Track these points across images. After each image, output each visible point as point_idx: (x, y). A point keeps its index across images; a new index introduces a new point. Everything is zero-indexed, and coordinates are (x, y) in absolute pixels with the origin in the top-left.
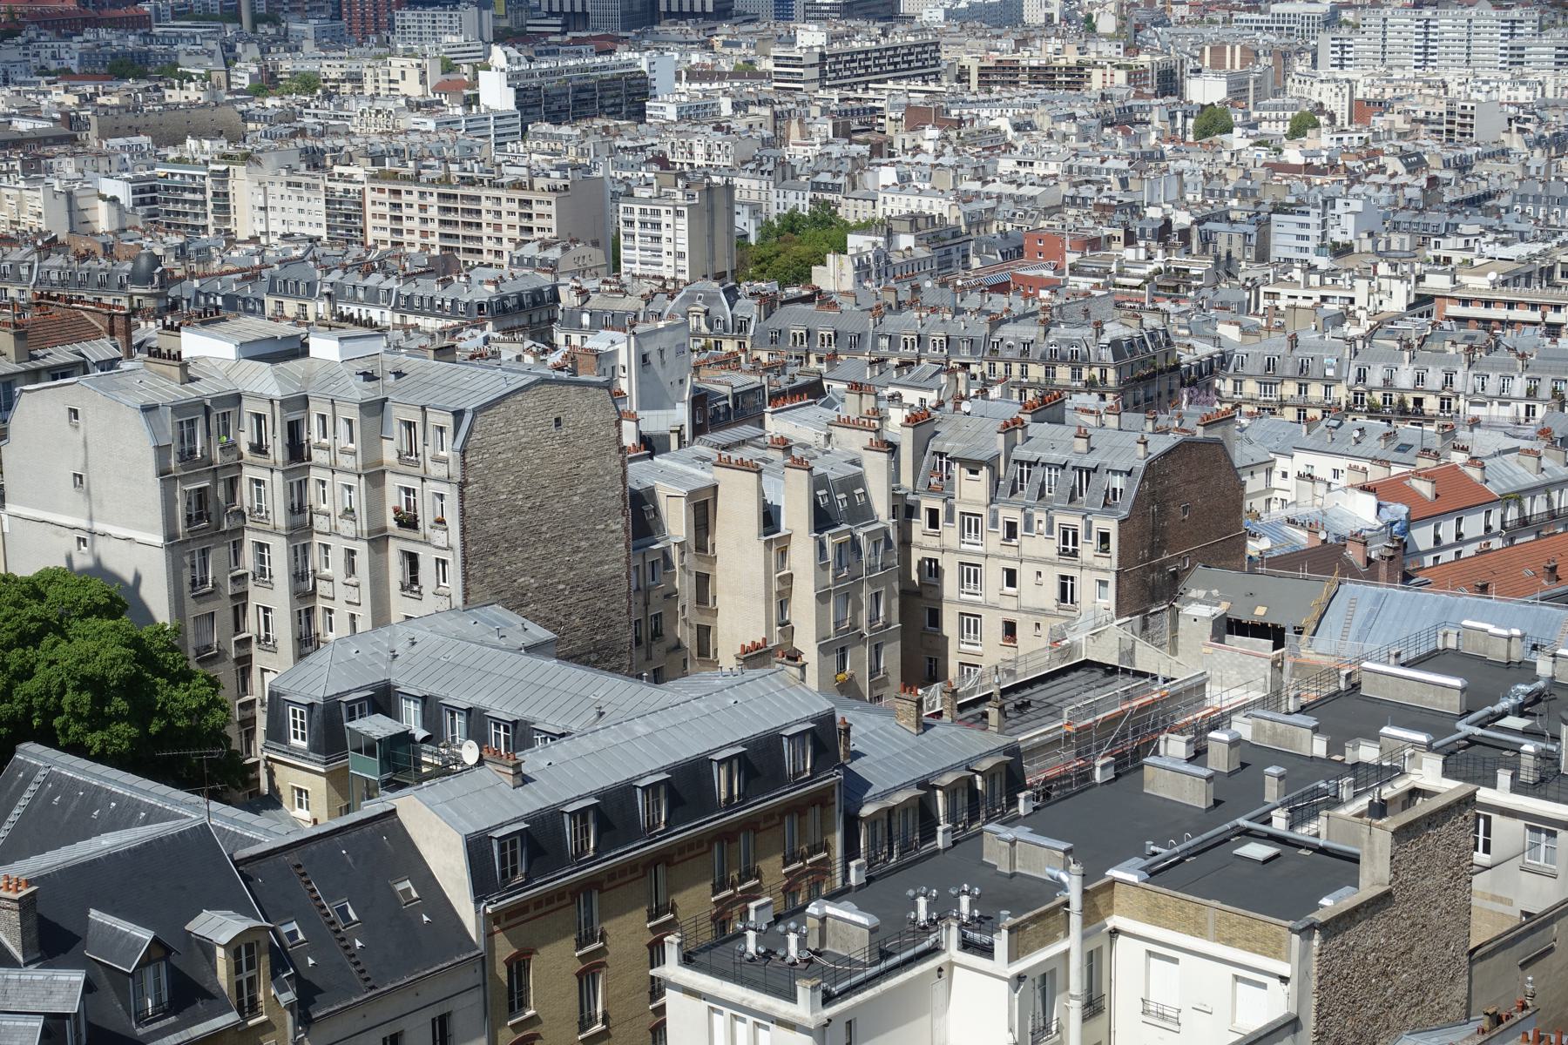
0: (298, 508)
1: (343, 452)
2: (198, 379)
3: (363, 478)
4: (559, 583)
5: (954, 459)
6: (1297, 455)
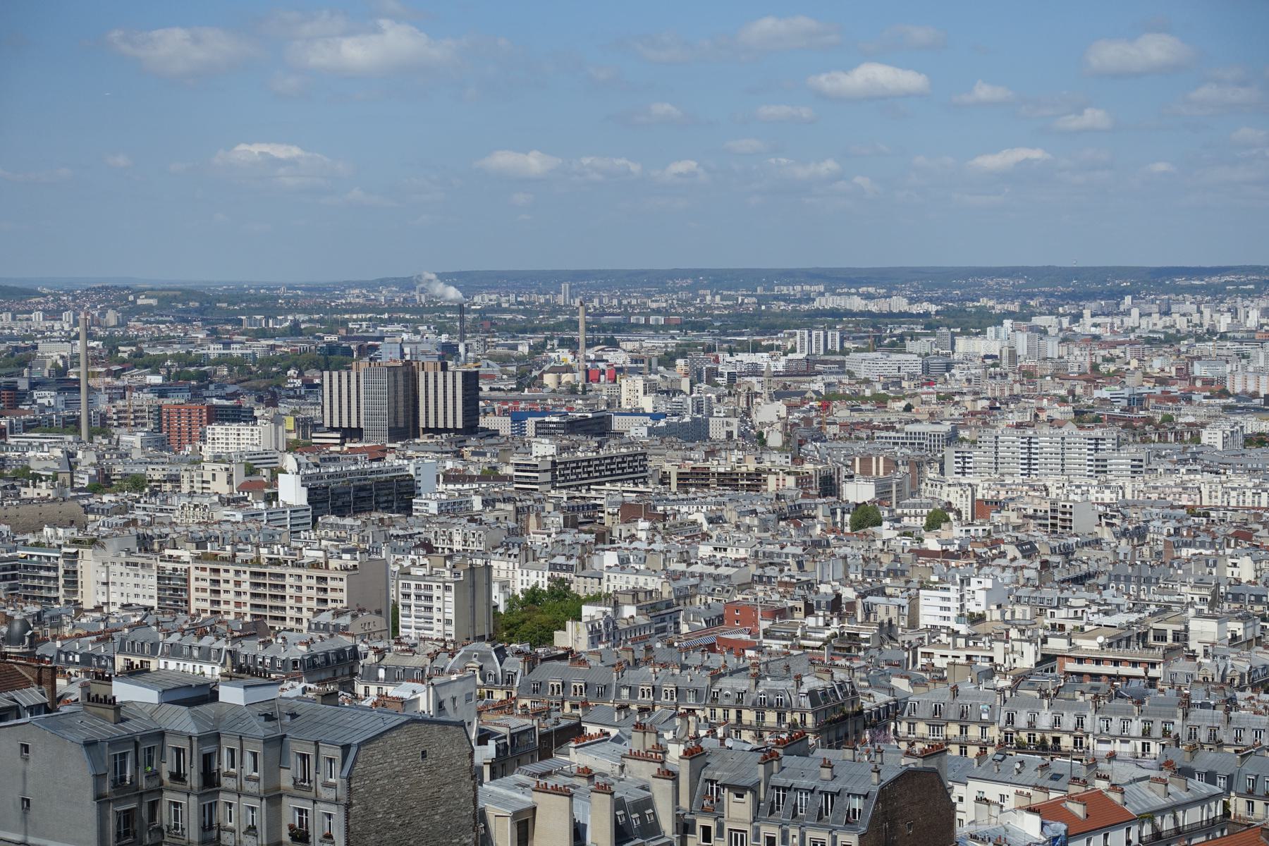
1: (249, 779)
2: (128, 720)
3: (264, 801)
5: (723, 786)
6: (971, 783)
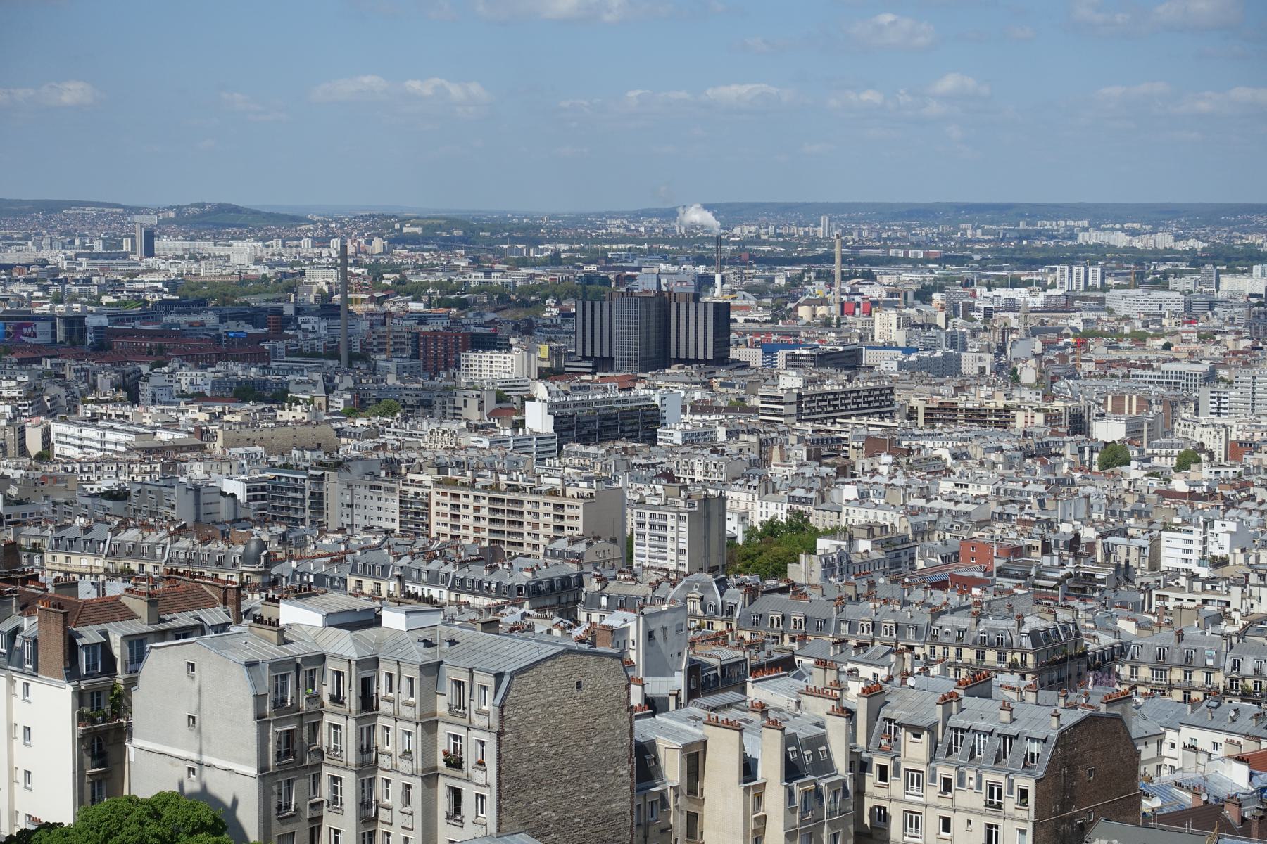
0: (366, 749)
2: (292, 642)
3: (420, 726)
4: (575, 817)
5: (901, 725)
6: (1183, 729)
